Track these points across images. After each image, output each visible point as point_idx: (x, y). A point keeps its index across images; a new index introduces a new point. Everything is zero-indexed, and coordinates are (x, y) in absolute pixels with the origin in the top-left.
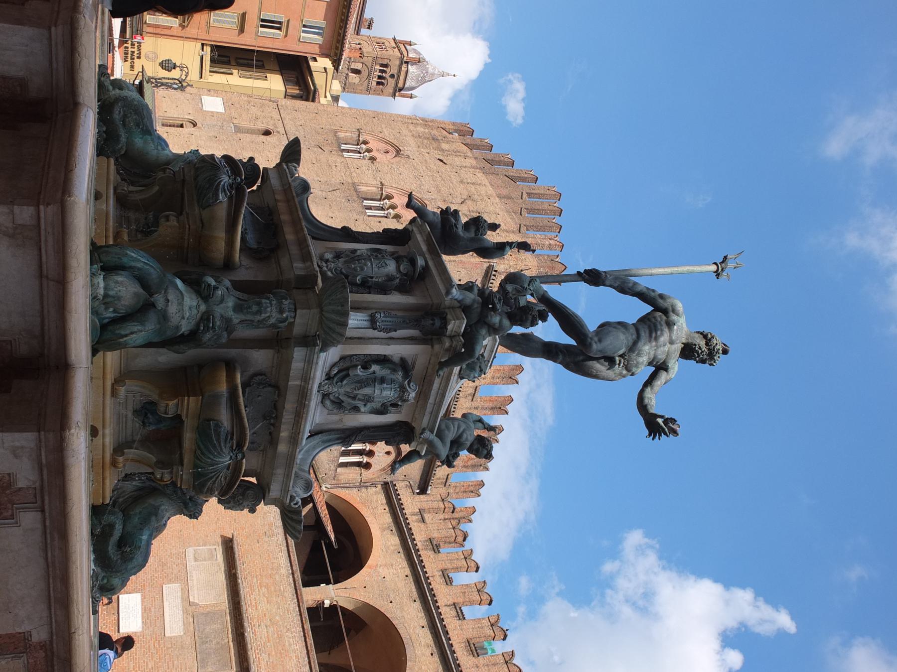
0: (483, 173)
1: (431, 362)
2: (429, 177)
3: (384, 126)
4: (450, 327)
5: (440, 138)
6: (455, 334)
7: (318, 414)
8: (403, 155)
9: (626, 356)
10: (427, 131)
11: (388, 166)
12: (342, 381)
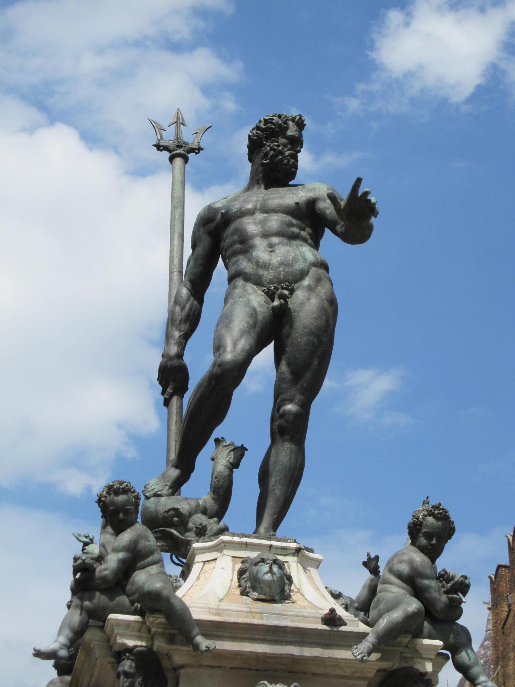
1: (215, 663)
4: (131, 643)
9: (269, 290)
10: (512, 653)
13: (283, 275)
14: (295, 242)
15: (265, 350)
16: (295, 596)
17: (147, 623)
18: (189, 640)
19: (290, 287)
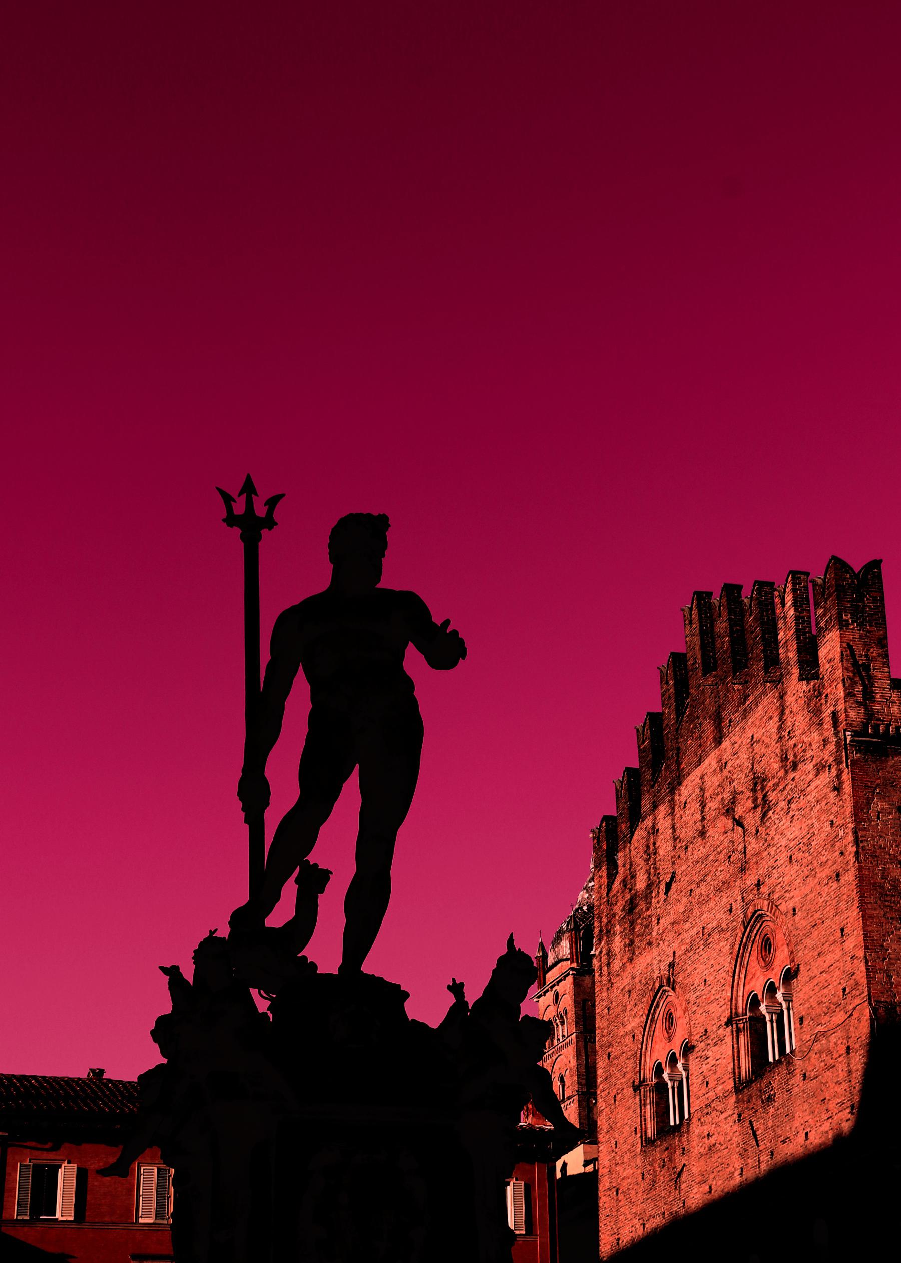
0: (680, 784)
2: (702, 914)
3: (622, 1032)
5: (628, 897)
8: (668, 979)
10: (618, 927)
11: (694, 1012)
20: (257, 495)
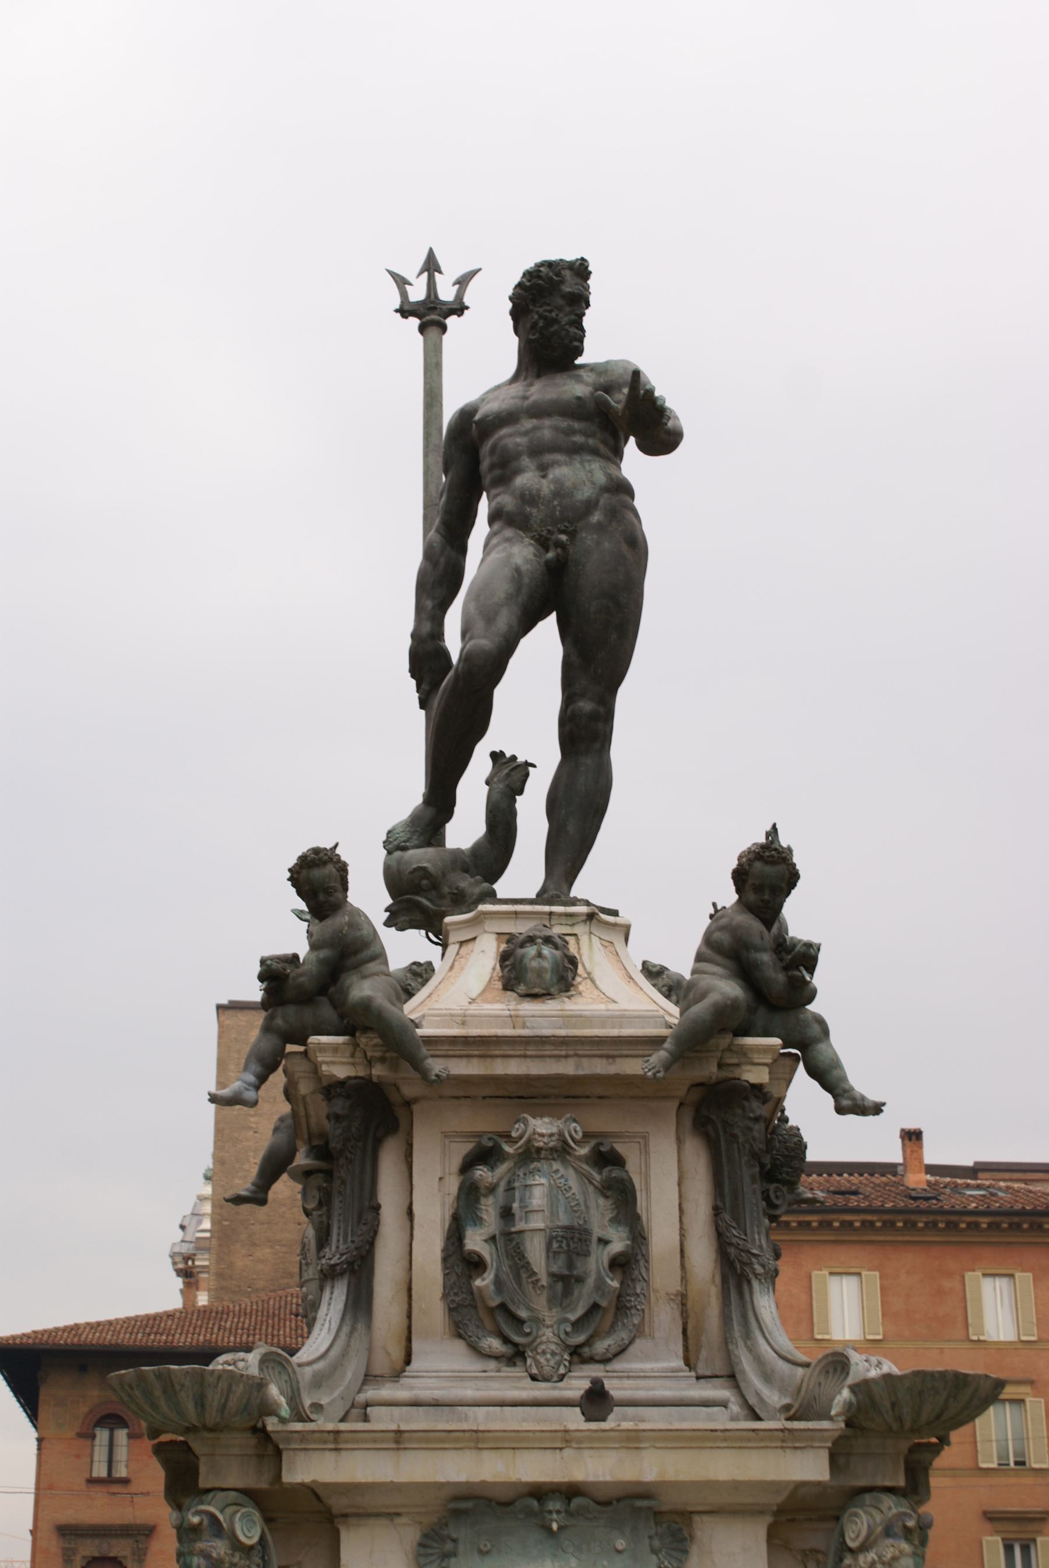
1: (461, 1093)
6: (358, 1054)
7: (648, 1366)
12: (520, 1322)
13: (560, 511)
14: (578, 458)
15: (541, 625)
16: (584, 986)
17: (362, 1046)
18: (417, 1065)
19: (571, 529)
20: (440, 272)
